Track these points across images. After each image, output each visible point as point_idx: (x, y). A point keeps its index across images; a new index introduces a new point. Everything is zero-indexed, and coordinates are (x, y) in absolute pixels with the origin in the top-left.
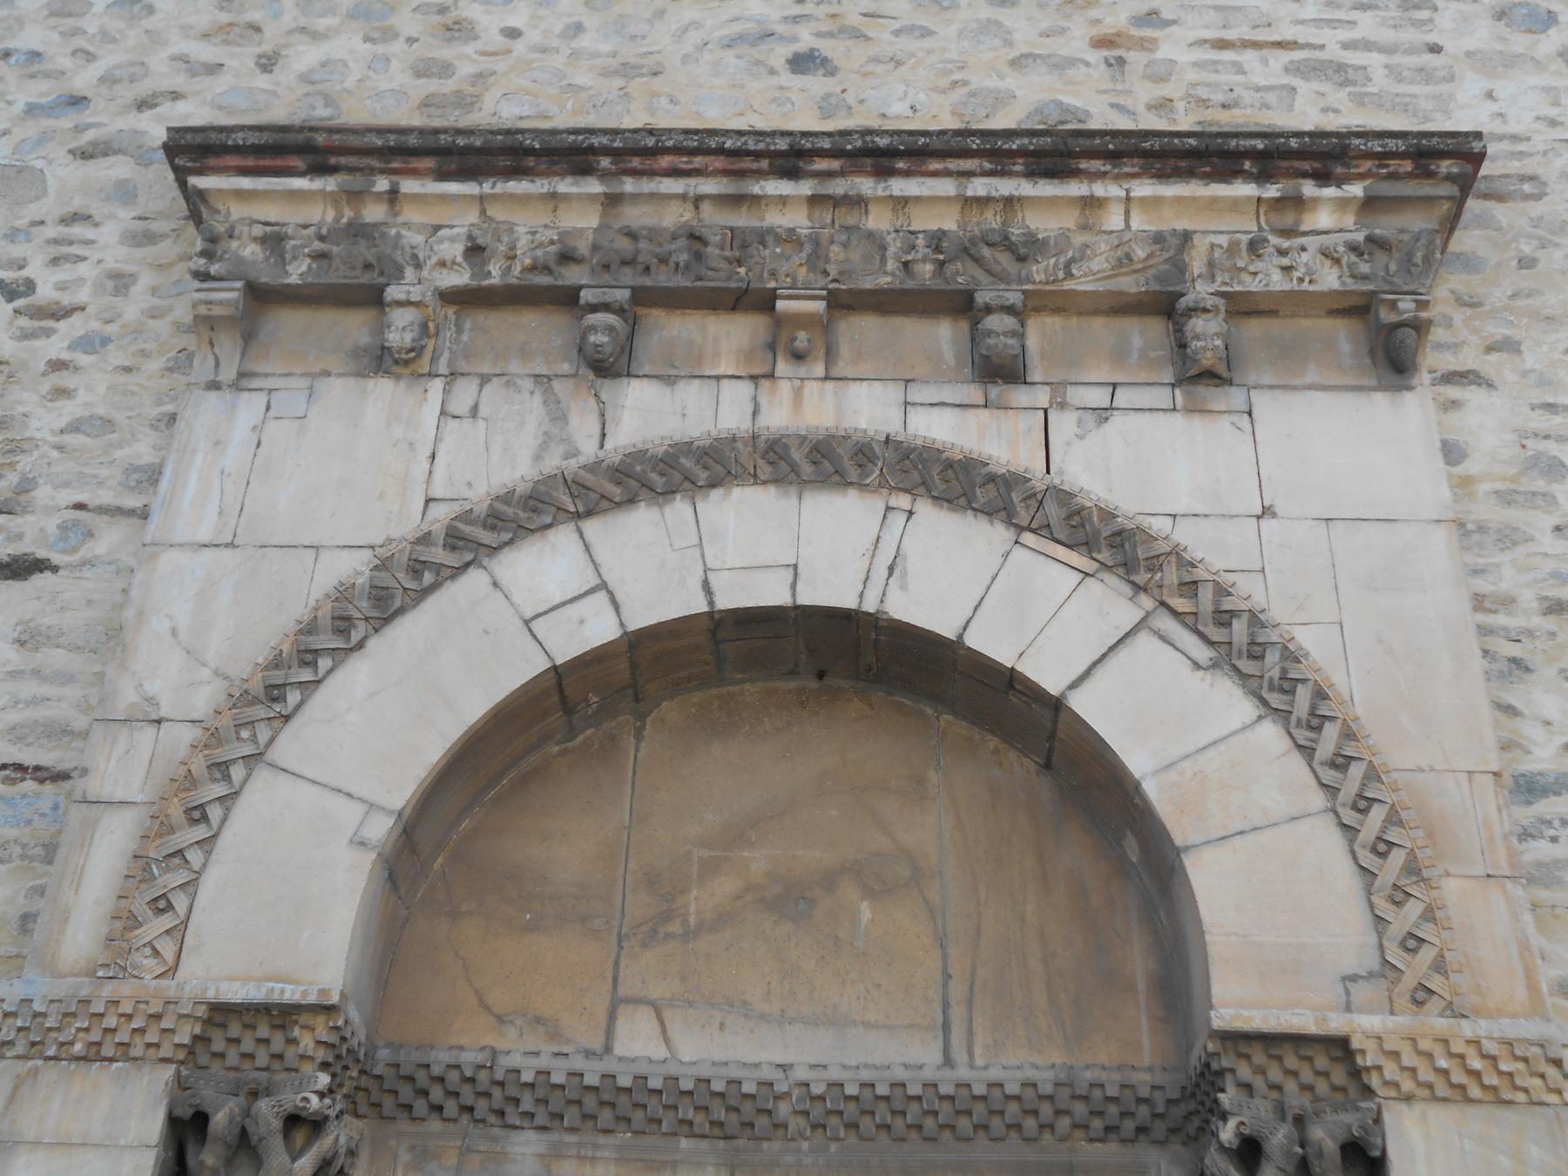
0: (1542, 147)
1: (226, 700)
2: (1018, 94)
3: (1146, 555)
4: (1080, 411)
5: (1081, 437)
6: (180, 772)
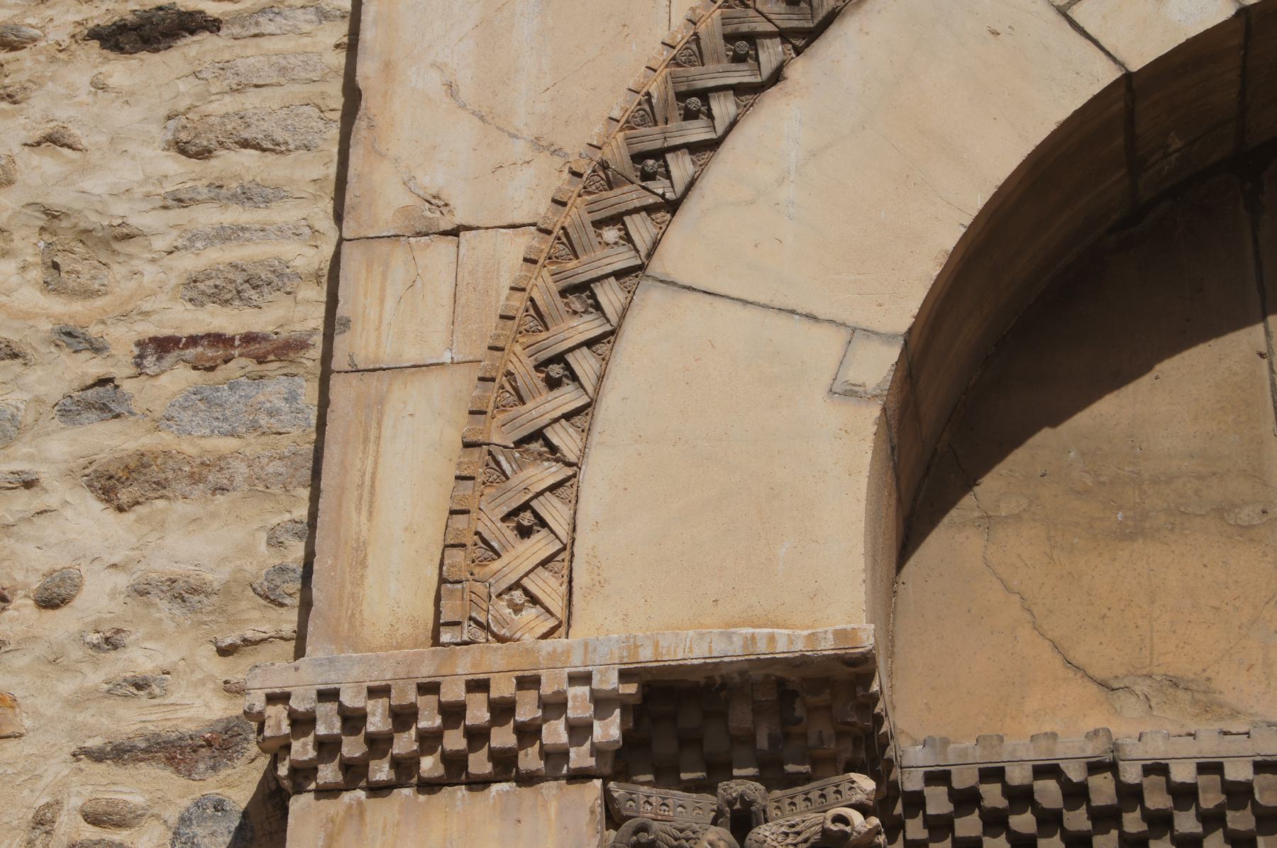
1: (570, 182)
6: (517, 304)
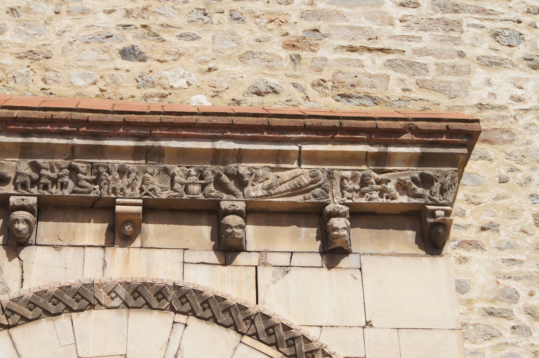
0: (513, 113)
2: (244, 75)
3: (307, 350)
4: (274, 267)
5: (275, 283)
